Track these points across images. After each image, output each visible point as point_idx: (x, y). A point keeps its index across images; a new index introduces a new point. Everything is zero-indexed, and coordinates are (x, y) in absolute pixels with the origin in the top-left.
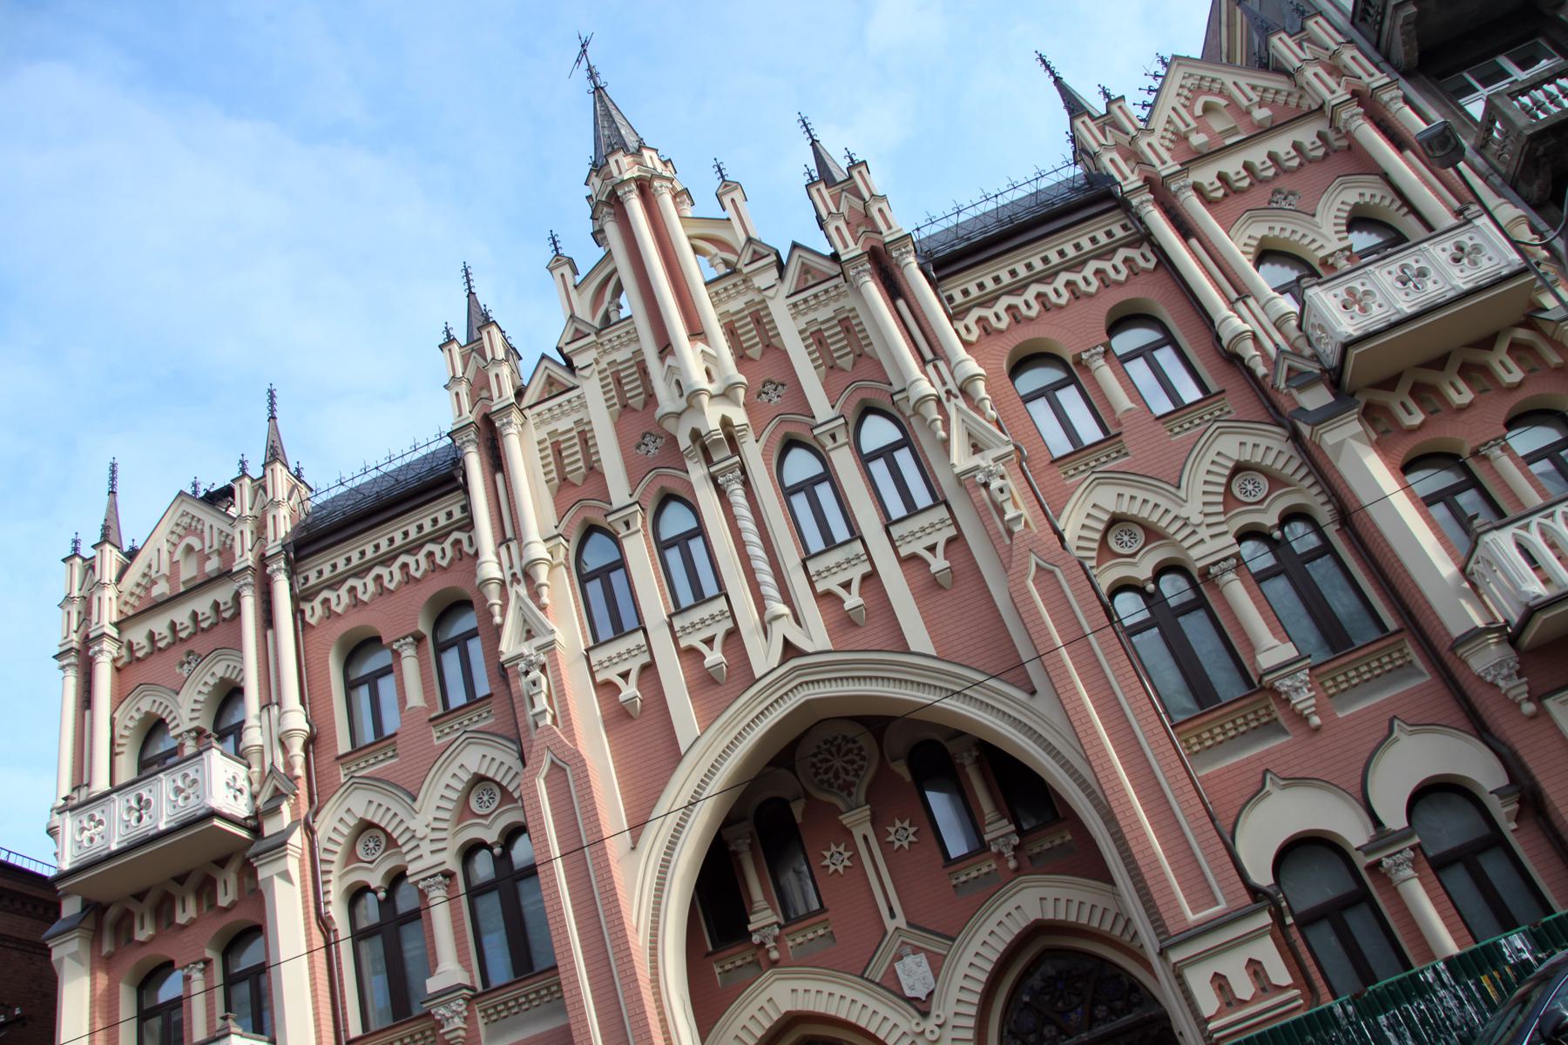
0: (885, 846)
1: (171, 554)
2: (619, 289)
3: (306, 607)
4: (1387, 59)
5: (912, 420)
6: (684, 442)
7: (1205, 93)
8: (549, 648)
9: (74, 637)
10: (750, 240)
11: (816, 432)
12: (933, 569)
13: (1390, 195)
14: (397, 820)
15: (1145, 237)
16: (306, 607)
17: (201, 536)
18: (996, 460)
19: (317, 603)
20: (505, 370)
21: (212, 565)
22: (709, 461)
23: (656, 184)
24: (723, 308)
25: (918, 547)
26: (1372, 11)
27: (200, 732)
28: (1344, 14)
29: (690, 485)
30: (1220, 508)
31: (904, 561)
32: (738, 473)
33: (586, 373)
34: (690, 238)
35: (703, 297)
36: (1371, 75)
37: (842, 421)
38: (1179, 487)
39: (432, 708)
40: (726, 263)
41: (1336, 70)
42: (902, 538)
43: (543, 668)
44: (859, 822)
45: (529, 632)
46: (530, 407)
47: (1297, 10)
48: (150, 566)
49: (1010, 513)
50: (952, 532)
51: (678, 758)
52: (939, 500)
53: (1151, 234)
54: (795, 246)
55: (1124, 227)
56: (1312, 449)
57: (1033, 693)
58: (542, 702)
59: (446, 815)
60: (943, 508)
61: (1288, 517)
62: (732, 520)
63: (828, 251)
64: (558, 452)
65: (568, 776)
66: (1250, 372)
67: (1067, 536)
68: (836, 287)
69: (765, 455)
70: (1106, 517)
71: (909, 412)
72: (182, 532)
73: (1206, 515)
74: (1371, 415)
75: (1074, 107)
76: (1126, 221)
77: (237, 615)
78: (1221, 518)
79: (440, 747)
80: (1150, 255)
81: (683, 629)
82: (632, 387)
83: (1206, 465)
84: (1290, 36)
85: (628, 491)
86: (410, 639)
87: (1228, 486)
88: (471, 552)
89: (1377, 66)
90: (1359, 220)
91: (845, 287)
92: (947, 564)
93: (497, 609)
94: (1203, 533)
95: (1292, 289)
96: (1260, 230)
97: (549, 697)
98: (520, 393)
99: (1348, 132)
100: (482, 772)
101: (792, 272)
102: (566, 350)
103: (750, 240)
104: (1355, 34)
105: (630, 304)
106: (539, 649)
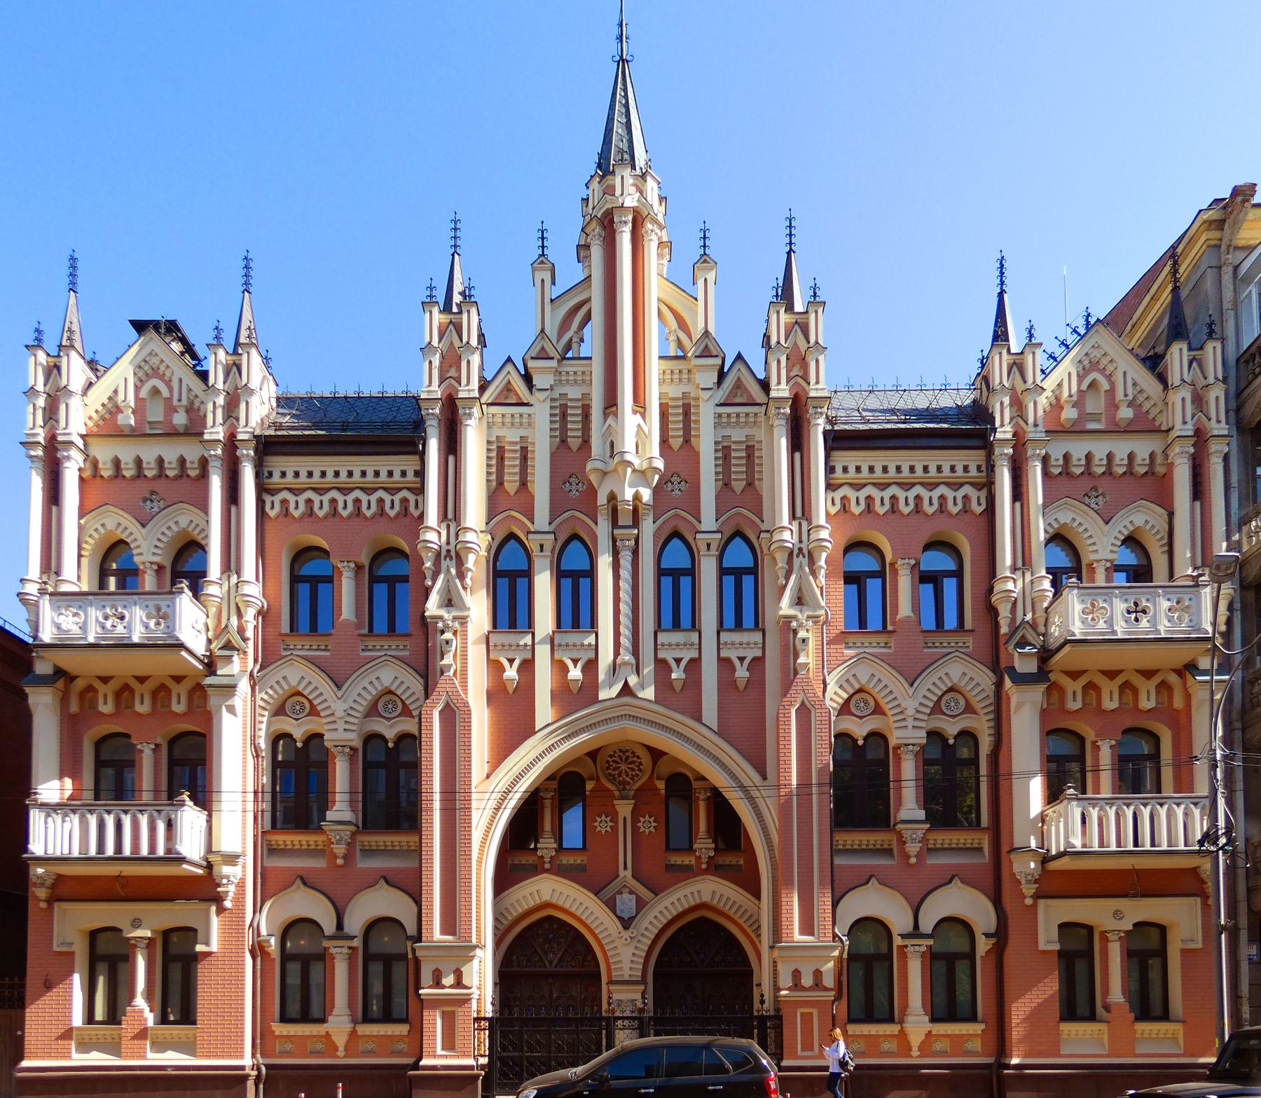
0: (635, 829)
1: (137, 389)
2: (588, 318)
3: (268, 499)
4: (1239, 409)
5: (766, 558)
6: (602, 499)
7: (1099, 371)
8: (463, 621)
9: (40, 431)
10: (706, 333)
11: (698, 536)
12: (738, 674)
13: (1164, 533)
14: (321, 699)
15: (988, 485)
16: (268, 499)
17: (168, 384)
18: (809, 617)
19: (277, 499)
20: (476, 359)
21: (180, 419)
22: (615, 524)
23: (649, 226)
24: (666, 389)
25: (733, 655)
26: (1257, 360)
27: (160, 569)
28: (1238, 347)
29: (595, 538)
30: (928, 711)
31: (720, 659)
32: (633, 542)
33: (542, 395)
34: (659, 300)
35: (654, 368)
36: (1219, 422)
37: (719, 536)
38: (912, 685)
39: (359, 626)
40: (680, 345)
41: (1199, 401)
42: (726, 643)
43: (455, 633)
44: (624, 809)
45: (450, 600)
46: (488, 405)
47: (1210, 325)
48: (116, 392)
49: (801, 660)
50: (759, 654)
51: (531, 732)
52: (758, 626)
53: (993, 483)
54: (739, 357)
55: (979, 468)
56: (1004, 698)
57: (764, 778)
58: (448, 660)
59: (361, 709)
60: (760, 634)
61: (967, 736)
62: (617, 577)
63: (761, 376)
64: (501, 458)
65: (454, 717)
66: (997, 626)
67: (829, 687)
68: (756, 414)
69: (656, 535)
70: (857, 686)
71: (765, 551)
72: (150, 372)
73: (918, 711)
74: (1054, 690)
75: (1000, 336)
76: (984, 464)
77: (204, 475)
78: (926, 718)
79: (365, 658)
80: (983, 501)
81: (560, 645)
82: (574, 426)
83: (935, 678)
84: (1190, 349)
85: (547, 520)
86: (352, 565)
87: (940, 698)
88: (416, 513)
89: (1227, 412)
90: (1131, 541)
91: (762, 418)
92: (747, 674)
93: (429, 574)
94: (910, 722)
95: (1057, 576)
96: (1065, 516)
97: (455, 656)
98: (482, 389)
99: (1172, 464)
100: (393, 688)
101: (729, 382)
102: (531, 364)
103: (706, 333)
104: (1232, 373)
105: (592, 344)
106: (455, 618)
